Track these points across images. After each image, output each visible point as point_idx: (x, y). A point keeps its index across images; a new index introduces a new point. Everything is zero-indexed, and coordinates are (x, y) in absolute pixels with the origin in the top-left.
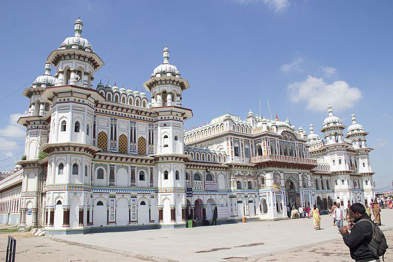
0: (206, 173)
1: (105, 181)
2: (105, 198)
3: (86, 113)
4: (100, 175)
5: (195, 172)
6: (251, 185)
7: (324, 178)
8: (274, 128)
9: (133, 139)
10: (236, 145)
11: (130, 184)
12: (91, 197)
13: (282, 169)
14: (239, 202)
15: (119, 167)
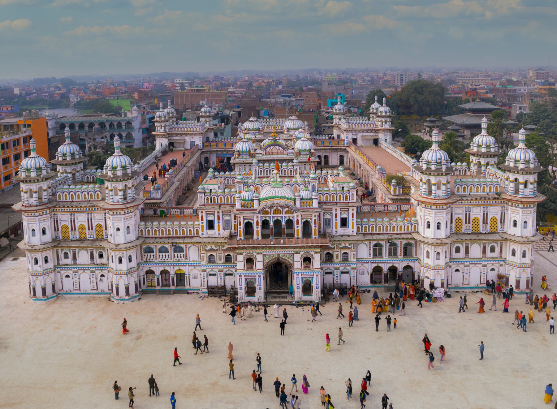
0: (173, 248)
1: (70, 261)
2: (70, 273)
3: (37, 222)
4: (66, 256)
5: (159, 246)
6: (231, 258)
7: (398, 242)
8: (256, 203)
9: (90, 227)
10: (210, 218)
11: (90, 262)
12: (59, 272)
13: (258, 251)
14: (211, 275)
15: (79, 250)
